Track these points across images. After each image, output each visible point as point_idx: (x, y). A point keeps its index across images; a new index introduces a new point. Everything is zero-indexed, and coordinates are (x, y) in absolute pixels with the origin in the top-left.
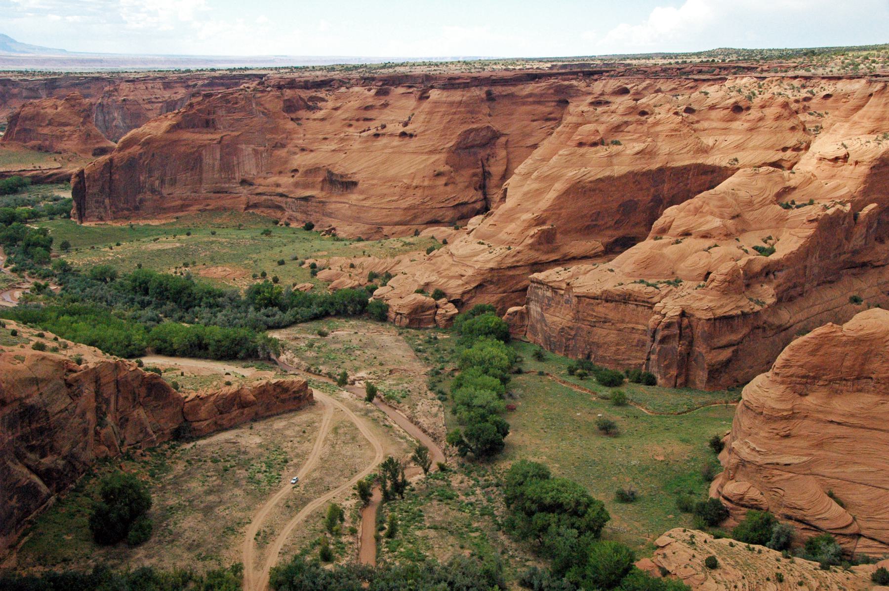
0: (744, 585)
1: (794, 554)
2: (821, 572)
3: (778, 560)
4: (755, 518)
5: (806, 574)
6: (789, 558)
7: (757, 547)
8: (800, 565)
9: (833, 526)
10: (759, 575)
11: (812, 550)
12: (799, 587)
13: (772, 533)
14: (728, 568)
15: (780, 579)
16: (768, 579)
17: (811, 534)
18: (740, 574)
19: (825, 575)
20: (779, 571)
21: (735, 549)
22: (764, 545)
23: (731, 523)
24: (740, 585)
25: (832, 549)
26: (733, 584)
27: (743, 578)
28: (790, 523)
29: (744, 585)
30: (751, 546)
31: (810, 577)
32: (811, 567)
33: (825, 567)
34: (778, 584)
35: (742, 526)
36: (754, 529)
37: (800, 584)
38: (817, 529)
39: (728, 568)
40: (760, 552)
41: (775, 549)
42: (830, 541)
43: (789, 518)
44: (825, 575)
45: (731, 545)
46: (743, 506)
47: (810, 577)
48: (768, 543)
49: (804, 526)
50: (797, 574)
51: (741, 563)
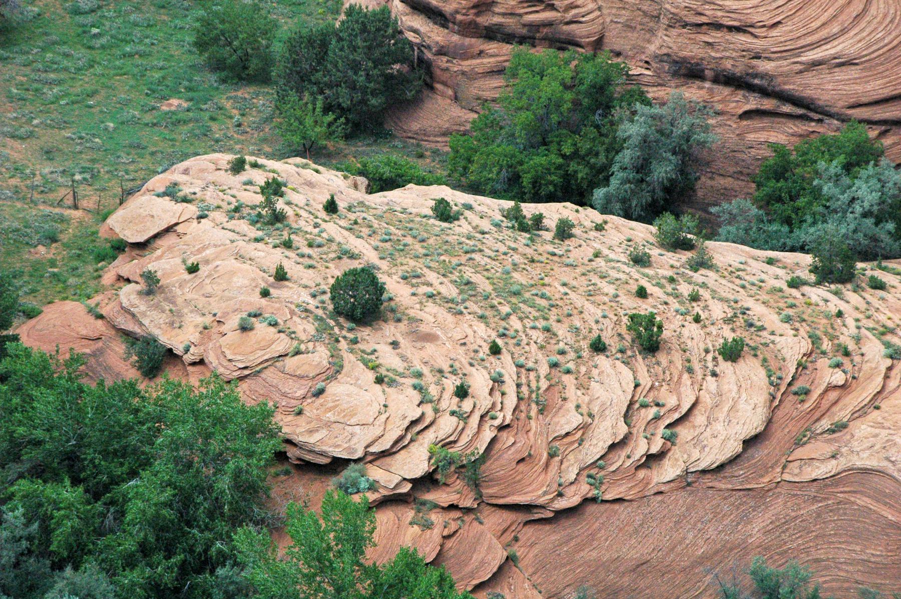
0: (498, 380)
1: (710, 229)
2: (816, 294)
3: (640, 260)
4: (550, 88)
5: (757, 310)
6: (686, 245)
7: (554, 212)
8: (734, 273)
9: (876, 88)
10: (561, 331)
11: (782, 205)
12: (725, 367)
13: (615, 148)
14: (432, 315)
15: (648, 340)
16: (598, 347)
17: (781, 134)
18: (482, 334)
19: (835, 304)
20: (644, 308)
21: (462, 227)
22: (581, 199)
23: (440, 114)
24: (480, 382)
25: (866, 191)
26: (451, 383)
27: (495, 350)
28: (694, 93)
29: (498, 380)
30: (529, 209)
31: (771, 319)
32: (776, 277)
33: (835, 271)
34: (640, 363)
35: (490, 127)
36: (540, 138)
37: (732, 353)
38: (808, 108)
39: (432, 315)
40: (564, 231)
41: (628, 216)
42: (859, 158)
43: (691, 72)
44: (835, 304)
45: (443, 212)
46: (491, 34)
47: (771, 319)
48: (599, 194)
49: (753, 102)
50: (718, 310)
51: (485, 286)
